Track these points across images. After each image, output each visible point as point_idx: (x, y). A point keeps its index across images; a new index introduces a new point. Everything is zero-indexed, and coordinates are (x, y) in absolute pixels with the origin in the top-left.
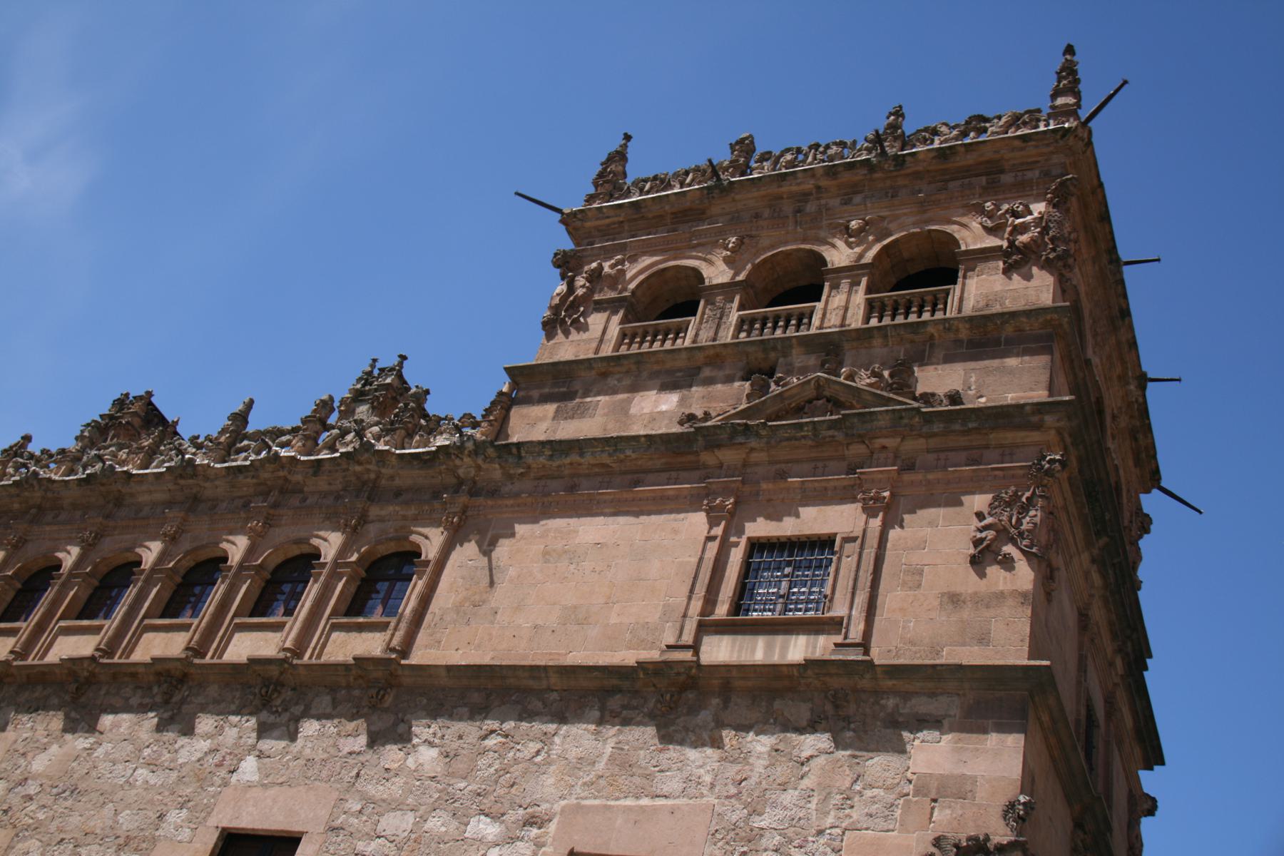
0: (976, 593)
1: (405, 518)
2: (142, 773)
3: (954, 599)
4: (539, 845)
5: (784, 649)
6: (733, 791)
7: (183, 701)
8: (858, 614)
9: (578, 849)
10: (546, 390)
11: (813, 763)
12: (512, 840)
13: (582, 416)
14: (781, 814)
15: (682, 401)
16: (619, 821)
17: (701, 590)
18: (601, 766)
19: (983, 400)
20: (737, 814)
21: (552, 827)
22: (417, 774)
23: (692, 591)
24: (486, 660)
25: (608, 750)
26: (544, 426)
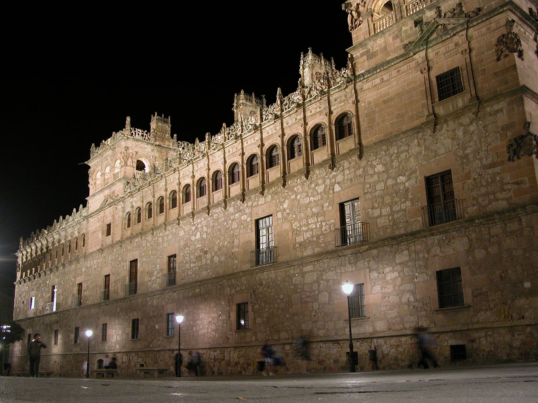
0: (501, 70)
1: (341, 106)
2: (312, 198)
3: (495, 74)
4: (417, 178)
5: (457, 105)
6: (458, 147)
7: (311, 178)
8: (472, 88)
9: (426, 176)
10: (361, 52)
11: (475, 133)
12: (409, 179)
13: (375, 56)
14: (471, 149)
15: (402, 41)
16: (433, 164)
17: (429, 97)
18: (423, 153)
19: (486, 7)
20: (460, 153)
21: (418, 172)
22: (379, 173)
23: (427, 98)
24: (383, 138)
25: (423, 148)
26: (366, 63)
